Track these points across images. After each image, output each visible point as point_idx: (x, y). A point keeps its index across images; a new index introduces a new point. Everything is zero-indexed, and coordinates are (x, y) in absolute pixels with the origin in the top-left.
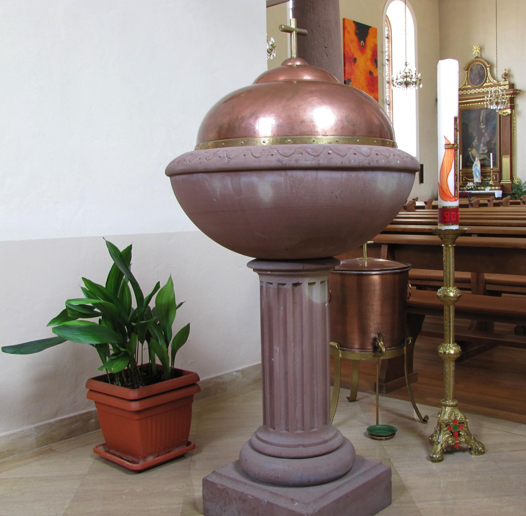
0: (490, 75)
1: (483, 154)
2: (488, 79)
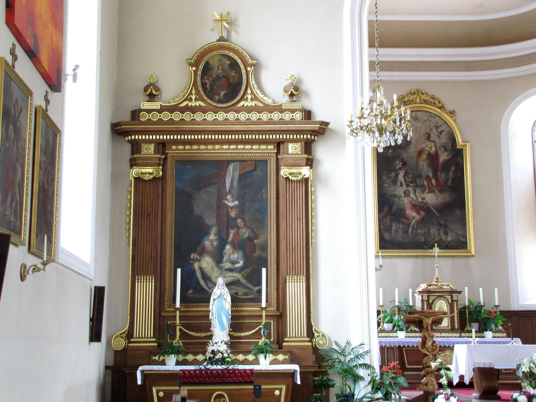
0: (254, 82)
1: (230, 270)
2: (249, 91)
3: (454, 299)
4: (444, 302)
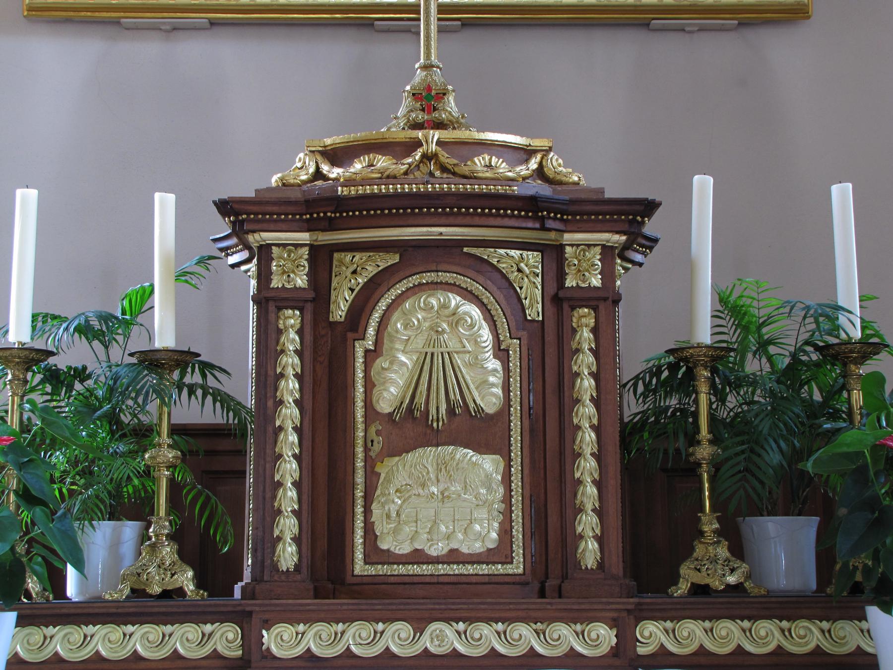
3: (570, 282)
4: (475, 312)
